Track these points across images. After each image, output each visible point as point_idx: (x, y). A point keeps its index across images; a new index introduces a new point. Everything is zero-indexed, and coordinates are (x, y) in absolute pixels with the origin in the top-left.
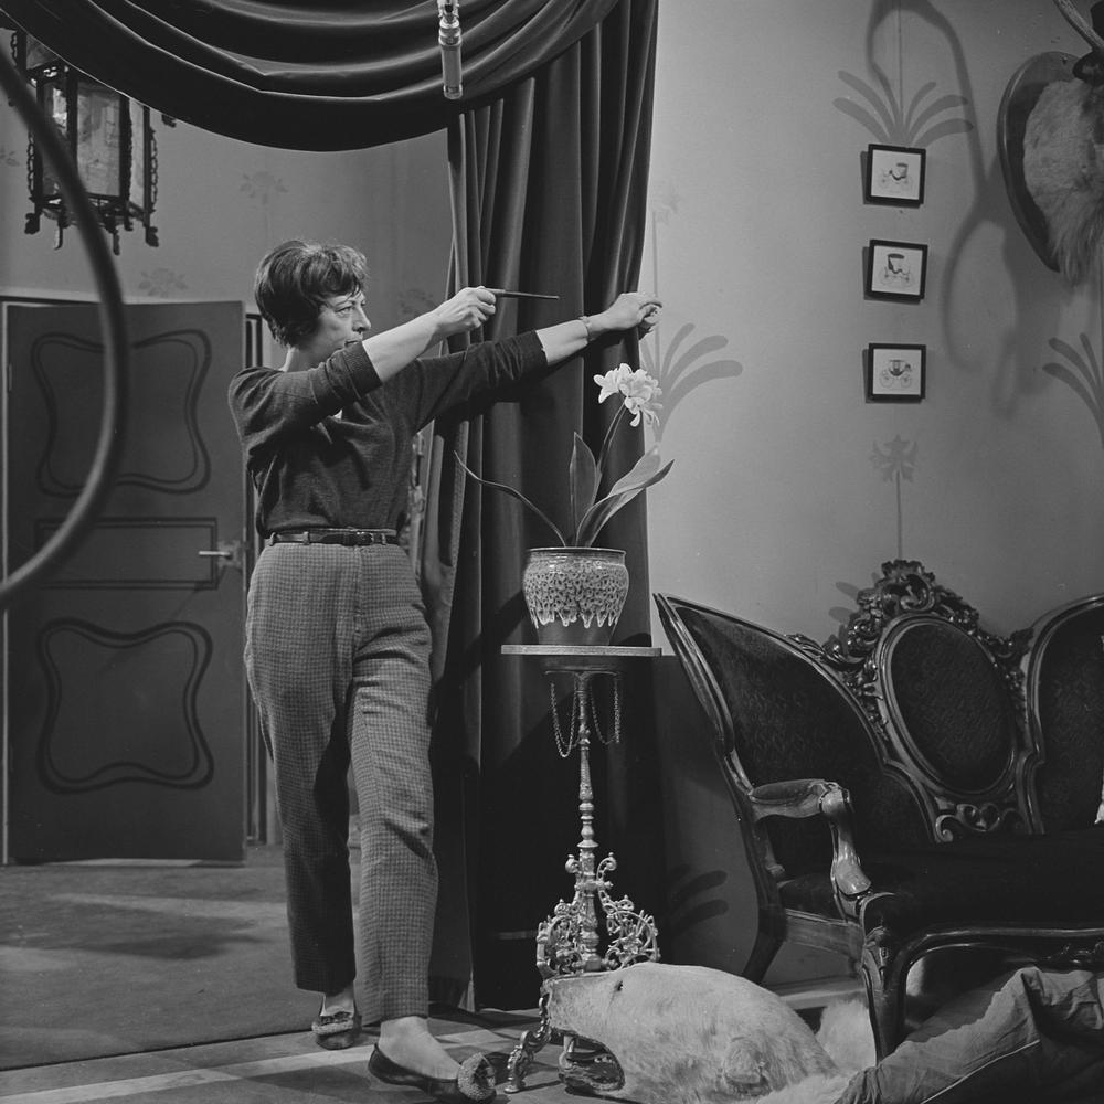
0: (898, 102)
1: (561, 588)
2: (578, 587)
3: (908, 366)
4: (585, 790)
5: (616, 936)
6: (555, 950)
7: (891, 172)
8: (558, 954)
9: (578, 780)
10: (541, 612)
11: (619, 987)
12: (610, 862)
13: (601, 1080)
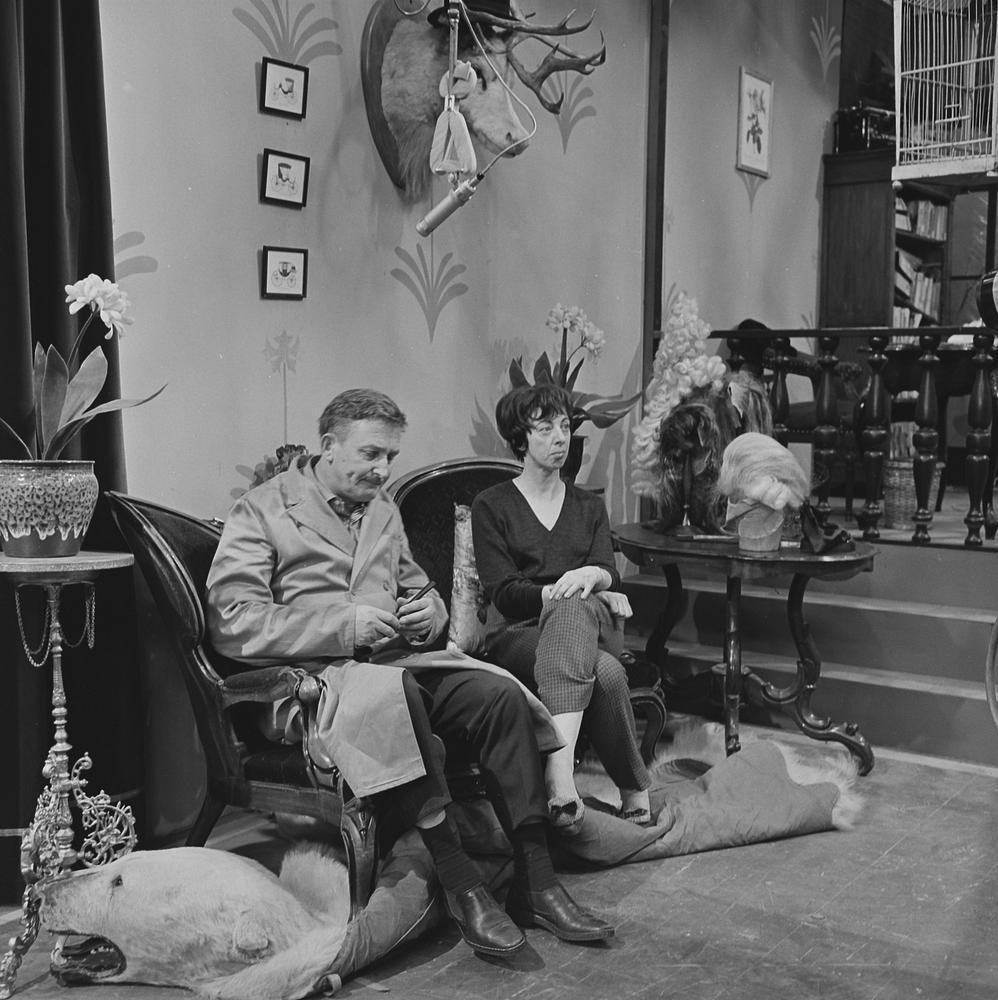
0: (284, 16)
1: (39, 502)
2: (58, 501)
3: (294, 268)
4: (58, 696)
5: (93, 829)
6: (37, 855)
7: (280, 86)
8: (42, 857)
9: (50, 686)
10: (15, 526)
11: (118, 882)
12: (86, 761)
13: (99, 969)
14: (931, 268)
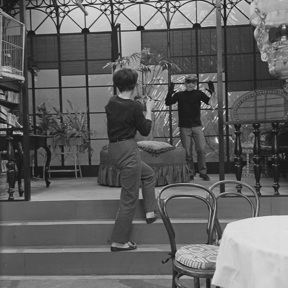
14: (16, 112)
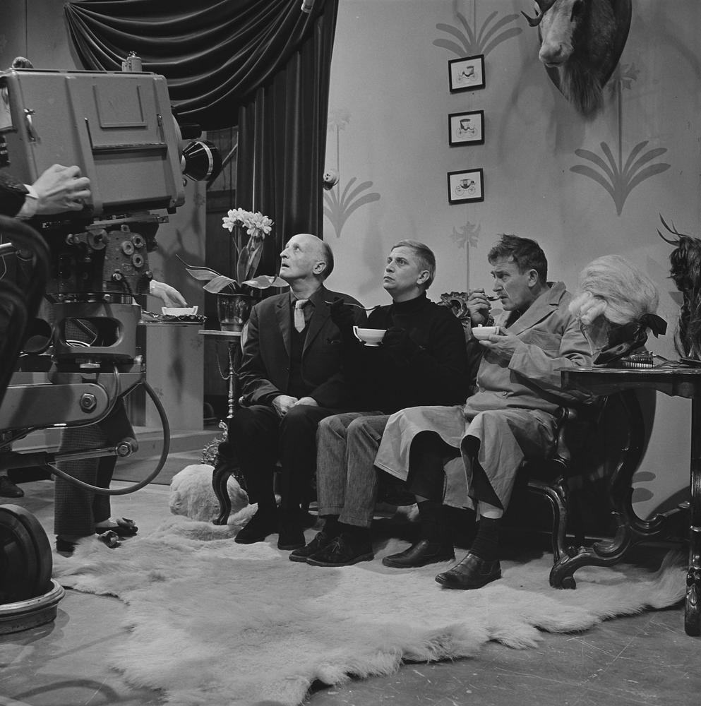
7: (464, 73)
